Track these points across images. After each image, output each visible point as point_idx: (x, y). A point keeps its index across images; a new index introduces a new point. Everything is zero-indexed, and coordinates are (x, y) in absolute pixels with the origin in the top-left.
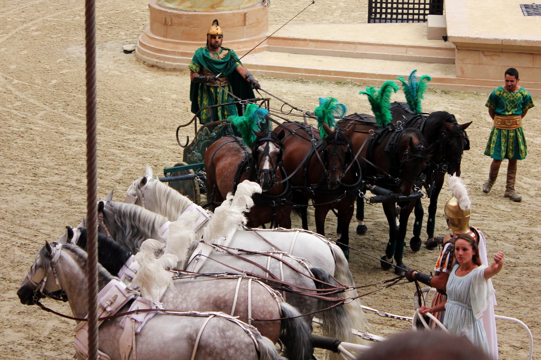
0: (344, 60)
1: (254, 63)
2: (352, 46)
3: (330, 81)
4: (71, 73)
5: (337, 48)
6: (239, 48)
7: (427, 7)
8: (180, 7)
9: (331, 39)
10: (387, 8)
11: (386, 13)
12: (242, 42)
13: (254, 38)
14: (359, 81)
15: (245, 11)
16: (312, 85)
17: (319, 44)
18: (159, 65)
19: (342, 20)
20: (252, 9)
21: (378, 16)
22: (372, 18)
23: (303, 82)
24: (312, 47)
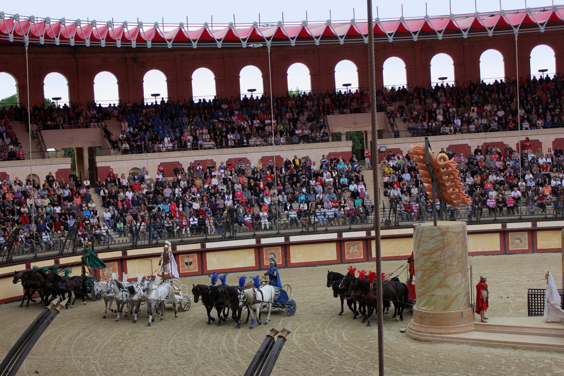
0: (516, 336)
2: (520, 328)
3: (509, 347)
4: (374, 342)
5: (512, 330)
8: (428, 309)
9: (508, 325)
11: (538, 311)
12: (461, 327)
13: (467, 324)
14: (525, 347)
16: (499, 349)
17: (502, 328)
18: (418, 338)
19: (514, 315)
21: (534, 313)
23: (494, 348)
24: (498, 329)
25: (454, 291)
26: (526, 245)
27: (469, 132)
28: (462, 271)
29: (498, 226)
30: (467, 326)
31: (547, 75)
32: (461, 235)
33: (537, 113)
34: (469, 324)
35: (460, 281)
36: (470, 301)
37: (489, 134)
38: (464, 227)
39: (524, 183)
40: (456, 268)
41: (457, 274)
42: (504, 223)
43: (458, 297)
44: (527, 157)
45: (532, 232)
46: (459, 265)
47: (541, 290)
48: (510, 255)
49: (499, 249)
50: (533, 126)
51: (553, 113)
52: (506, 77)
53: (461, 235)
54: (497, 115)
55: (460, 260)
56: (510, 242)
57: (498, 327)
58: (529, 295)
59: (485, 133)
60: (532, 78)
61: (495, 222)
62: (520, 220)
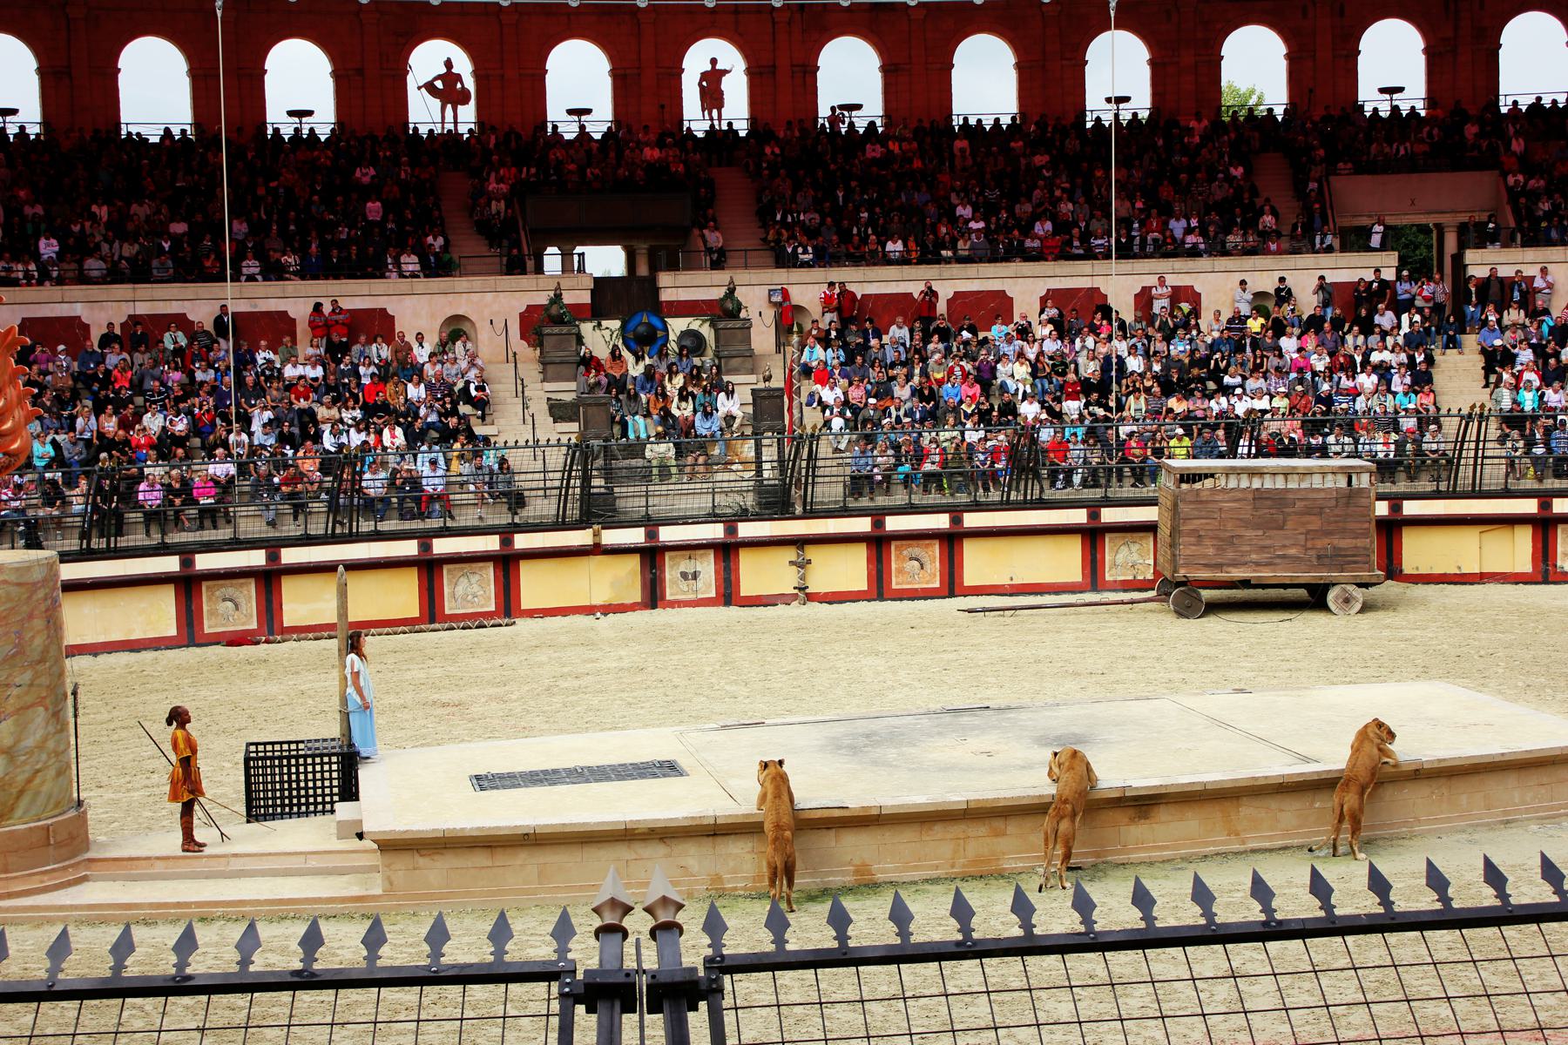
0: (211, 882)
1: (68, 903)
6: (42, 882)
7: (336, 790)
10: (323, 795)
14: (234, 913)
15: (49, 822)
17: (171, 863)
20: (60, 818)
22: (252, 816)
24: (159, 867)
25: (24, 763)
26: (251, 616)
27: (83, 279)
28: (48, 701)
29: (171, 564)
30: (65, 868)
31: (312, 130)
32: (41, 594)
33: (283, 232)
34: (72, 862)
35: (39, 734)
36: (75, 795)
37: (144, 290)
38: (51, 569)
39: (244, 437)
40: (27, 693)
41: (30, 711)
42: (187, 553)
43: (37, 781)
44: (254, 361)
45: (269, 580)
46: (36, 682)
47: (281, 743)
48: (205, 649)
49: (173, 632)
50: (274, 272)
51: (329, 237)
52: (197, 123)
53: (41, 594)
54: (169, 234)
55: (40, 667)
56: (205, 608)
57: (159, 863)
58: (247, 760)
59: (131, 286)
60: (270, 131)
61: (162, 550)
62: (236, 544)
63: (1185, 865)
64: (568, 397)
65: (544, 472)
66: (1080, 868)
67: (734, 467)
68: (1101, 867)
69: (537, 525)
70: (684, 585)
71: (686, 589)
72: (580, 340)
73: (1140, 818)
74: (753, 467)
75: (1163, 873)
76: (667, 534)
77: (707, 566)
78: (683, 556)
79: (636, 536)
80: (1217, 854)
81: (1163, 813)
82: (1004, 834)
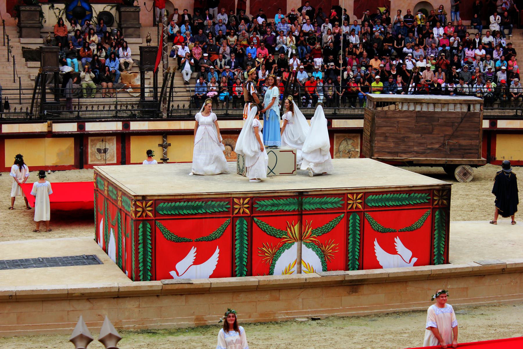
63: (376, 318)
64: (34, 47)
65: (20, 89)
66: (319, 319)
67: (128, 90)
68: (331, 318)
69: (15, 119)
70: (98, 156)
71: (100, 158)
72: (41, 14)
73: (353, 292)
74: (139, 90)
75: (365, 322)
76: (90, 127)
77: (112, 147)
78: (99, 140)
79: (72, 127)
80: (394, 313)
81: (365, 290)
82: (278, 300)
